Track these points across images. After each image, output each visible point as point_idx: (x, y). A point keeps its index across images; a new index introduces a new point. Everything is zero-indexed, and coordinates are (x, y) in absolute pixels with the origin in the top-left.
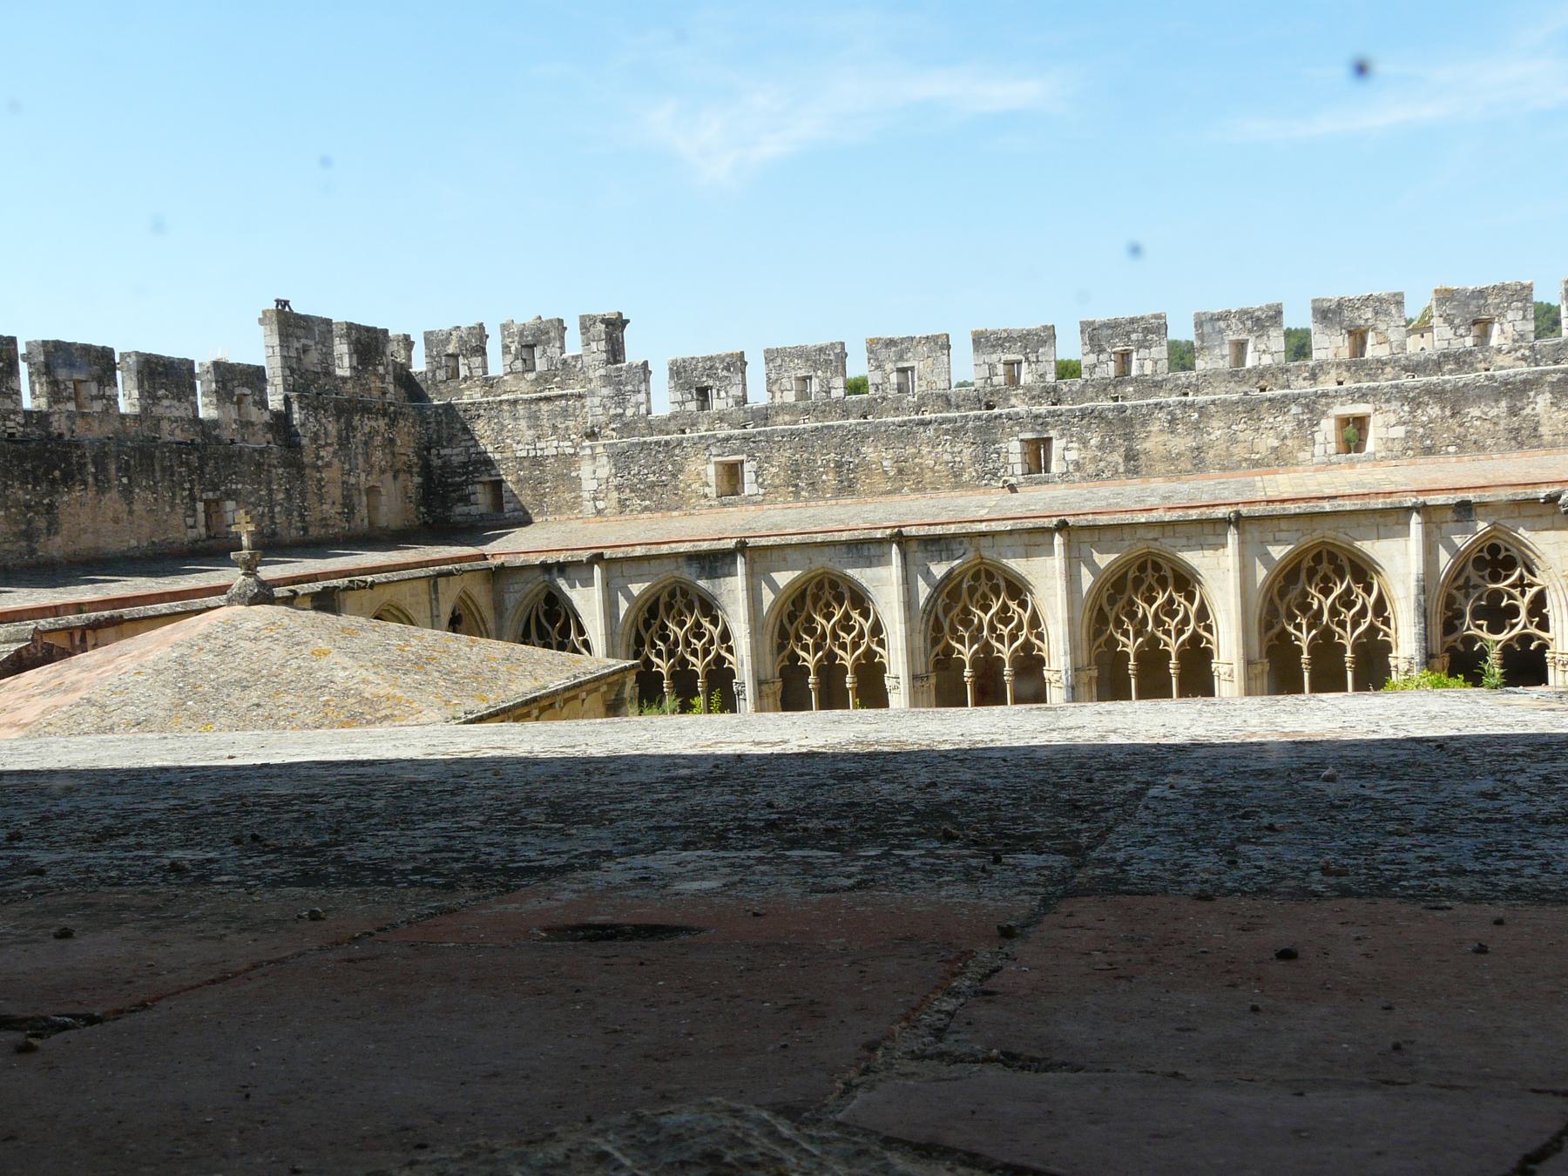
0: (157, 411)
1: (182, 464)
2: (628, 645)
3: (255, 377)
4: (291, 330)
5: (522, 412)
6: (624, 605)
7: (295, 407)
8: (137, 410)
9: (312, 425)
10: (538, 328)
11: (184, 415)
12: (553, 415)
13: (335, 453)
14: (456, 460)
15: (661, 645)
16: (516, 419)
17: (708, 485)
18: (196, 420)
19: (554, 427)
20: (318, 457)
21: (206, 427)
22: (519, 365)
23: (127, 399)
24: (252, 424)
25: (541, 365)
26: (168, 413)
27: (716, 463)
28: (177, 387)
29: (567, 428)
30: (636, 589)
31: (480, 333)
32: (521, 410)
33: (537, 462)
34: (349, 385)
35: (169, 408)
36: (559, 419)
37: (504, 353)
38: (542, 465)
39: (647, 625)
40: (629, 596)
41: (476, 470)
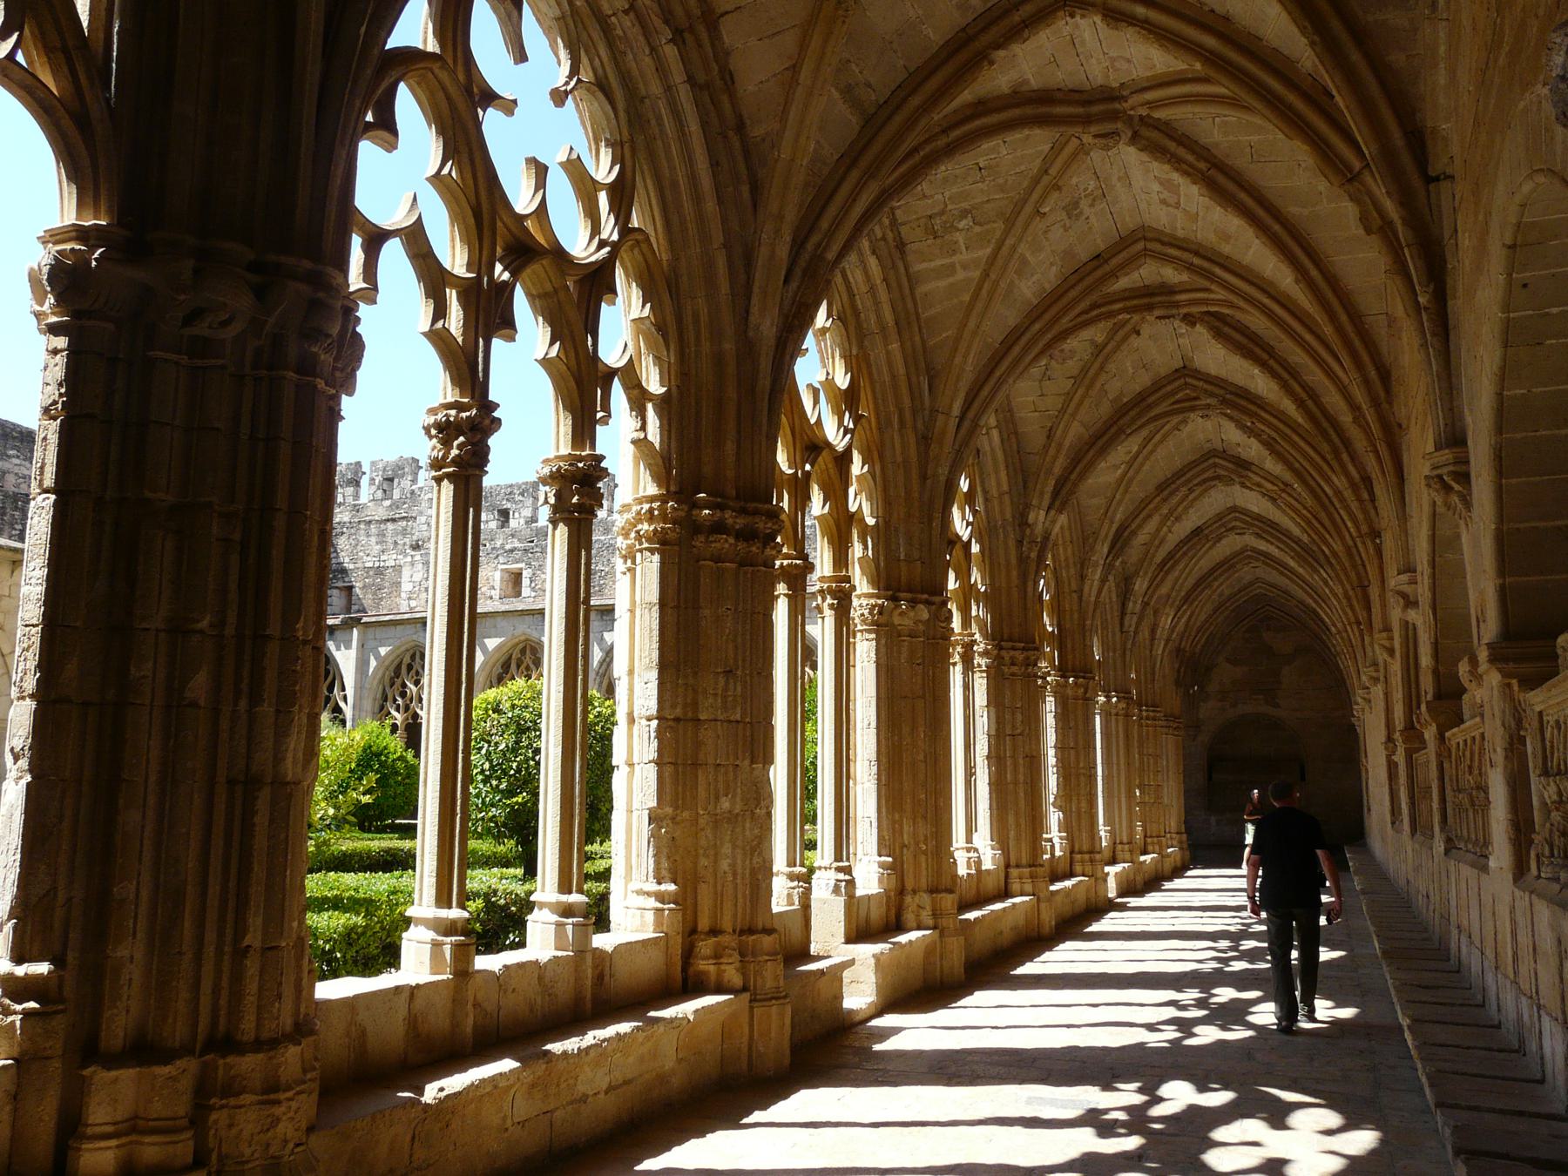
1: (16, 508)
2: (375, 700)
5: (373, 530)
6: (373, 663)
10: (397, 465)
15: (400, 701)
16: (368, 535)
17: (493, 588)
19: (396, 543)
22: (379, 494)
25: (396, 494)
27: (502, 570)
29: (405, 544)
30: (383, 651)
32: (373, 528)
33: (379, 571)
36: (400, 537)
37: (370, 484)
38: (382, 574)
39: (392, 685)
40: (377, 657)
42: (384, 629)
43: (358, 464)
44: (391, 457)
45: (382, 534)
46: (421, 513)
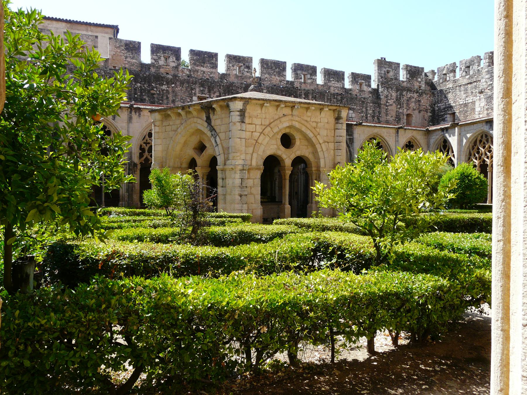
0: (329, 84)
1: (334, 98)
2: (466, 156)
3: (368, 78)
4: (382, 65)
6: (465, 141)
7: (380, 87)
8: (323, 84)
9: (386, 92)
11: (339, 86)
12: (472, 88)
13: (394, 102)
14: (442, 107)
15: (477, 155)
16: (460, 91)
18: (343, 88)
19: (472, 92)
20: (387, 102)
21: (347, 91)
22: (464, 74)
23: (320, 79)
24: (364, 91)
25: (471, 72)
26: (333, 85)
28: (338, 78)
29: (476, 92)
30: (469, 135)
31: (454, 65)
33: (466, 105)
34: (405, 83)
35: (334, 84)
39: (473, 149)
40: (466, 138)
41: (448, 110)
42: (469, 126)
43: (455, 63)
44: (468, 57)
45: (466, 90)
46: (483, 78)
